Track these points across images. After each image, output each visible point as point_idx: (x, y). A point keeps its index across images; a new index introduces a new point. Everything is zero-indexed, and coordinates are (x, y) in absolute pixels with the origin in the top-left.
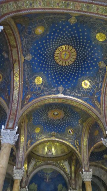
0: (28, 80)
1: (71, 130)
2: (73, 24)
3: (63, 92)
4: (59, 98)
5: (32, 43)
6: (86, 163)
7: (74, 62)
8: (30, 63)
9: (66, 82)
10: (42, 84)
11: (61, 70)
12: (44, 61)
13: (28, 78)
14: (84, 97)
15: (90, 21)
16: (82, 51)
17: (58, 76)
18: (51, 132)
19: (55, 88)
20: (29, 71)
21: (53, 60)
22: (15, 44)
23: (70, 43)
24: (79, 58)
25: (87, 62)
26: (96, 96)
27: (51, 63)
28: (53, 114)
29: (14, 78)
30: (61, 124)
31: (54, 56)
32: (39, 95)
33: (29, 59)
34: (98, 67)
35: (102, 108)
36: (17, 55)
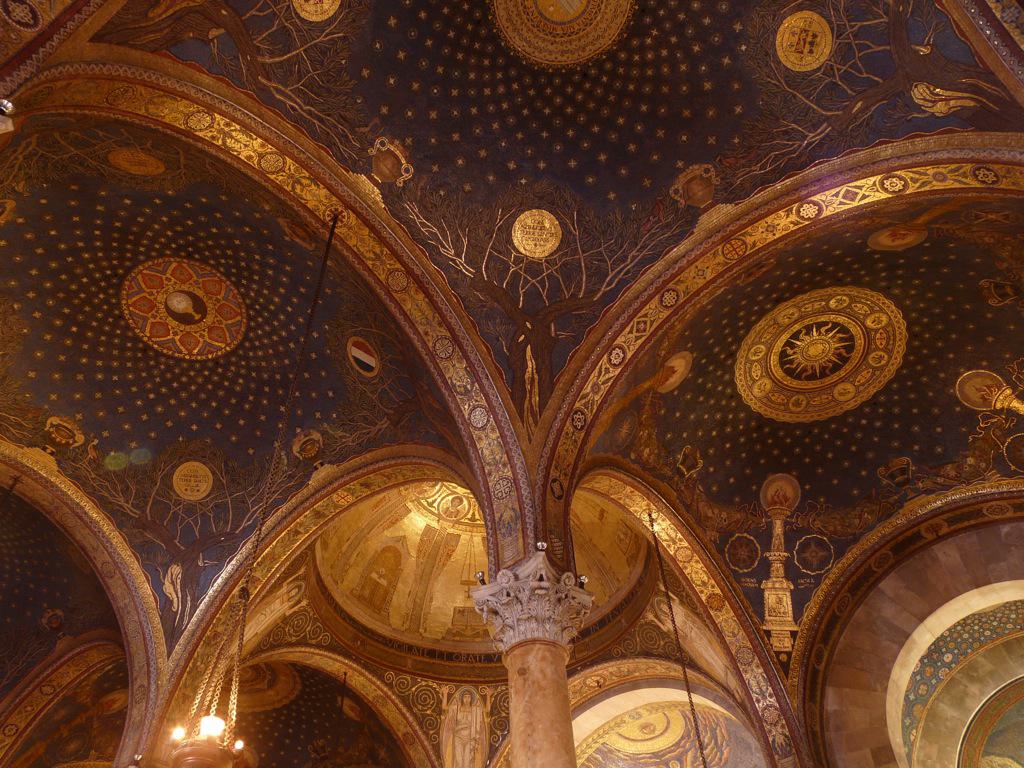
18: (287, 446)
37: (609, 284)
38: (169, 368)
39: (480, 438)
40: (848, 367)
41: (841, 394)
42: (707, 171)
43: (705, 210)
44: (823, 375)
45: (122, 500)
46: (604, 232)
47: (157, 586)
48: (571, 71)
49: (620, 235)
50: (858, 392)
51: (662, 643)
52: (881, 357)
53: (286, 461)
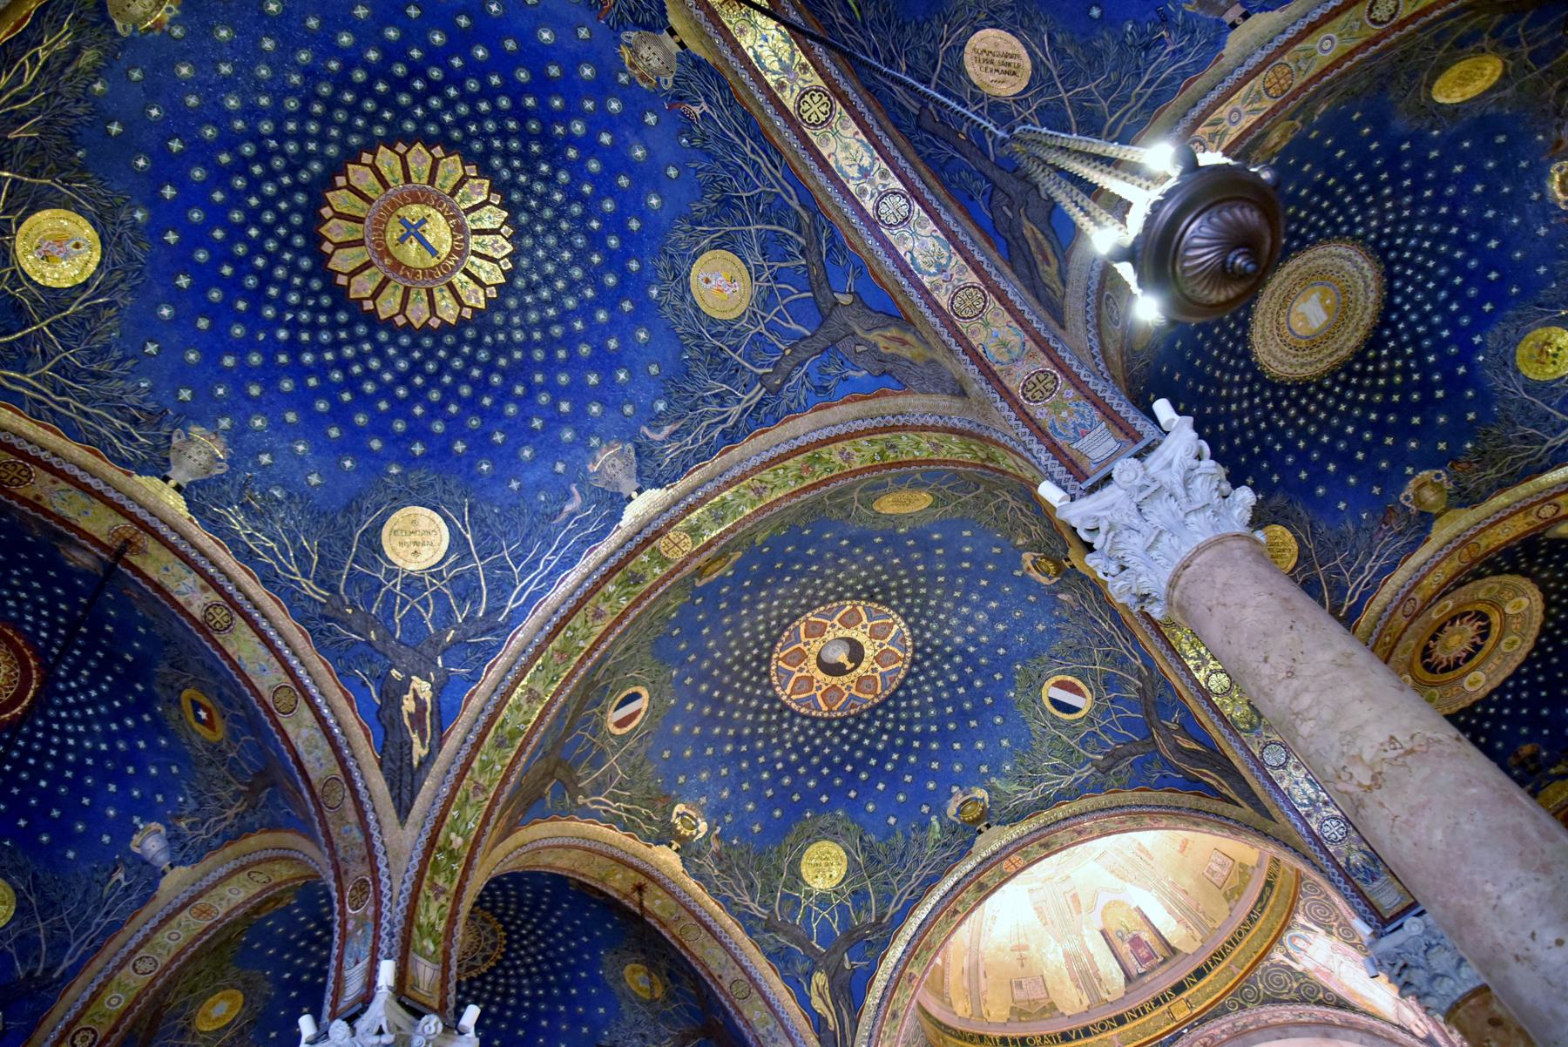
0: (333, 589)
1: (1061, 685)
3: (639, 473)
5: (117, 354)
6: (1357, 859)
9: (598, 395)
10: (457, 541)
11: (497, 350)
13: (321, 583)
14: (788, 379)
16: (463, 109)
17: (518, 400)
19: (568, 496)
21: (383, 336)
23: (342, 143)
24: (507, 165)
25: (570, 139)
26: (845, 299)
27: (388, 364)
28: (819, 675)
29: (230, 650)
30: (956, 701)
31: (360, 301)
32: (491, 630)
34: (652, 99)
36: (99, 506)
37: (1352, 598)
38: (803, 730)
39: (1282, 778)
40: (1479, 656)
41: (1471, 684)
42: (1438, 476)
43: (1439, 515)
44: (1457, 666)
45: (747, 898)
46: (1338, 544)
47: (804, 1002)
48: (1308, 383)
49: (1354, 546)
50: (1488, 680)
51: (1295, 985)
52: (1514, 642)
53: (938, 827)
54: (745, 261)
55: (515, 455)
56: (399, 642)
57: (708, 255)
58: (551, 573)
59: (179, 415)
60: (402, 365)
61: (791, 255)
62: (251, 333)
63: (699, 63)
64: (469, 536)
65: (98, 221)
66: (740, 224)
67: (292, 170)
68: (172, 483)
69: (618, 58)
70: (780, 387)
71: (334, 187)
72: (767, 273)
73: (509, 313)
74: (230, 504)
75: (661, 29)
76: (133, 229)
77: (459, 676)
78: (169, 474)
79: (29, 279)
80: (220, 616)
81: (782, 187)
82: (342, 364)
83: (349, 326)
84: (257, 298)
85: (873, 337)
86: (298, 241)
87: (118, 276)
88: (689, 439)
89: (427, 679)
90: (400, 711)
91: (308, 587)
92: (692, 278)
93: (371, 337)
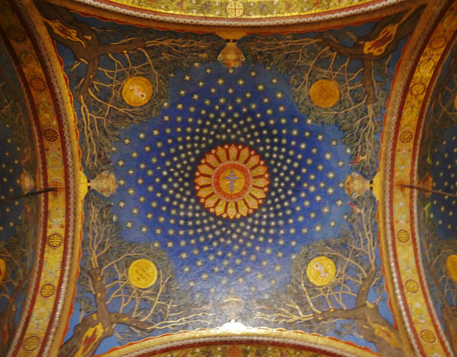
0: (101, 266)
2: (234, 68)
4: (226, 342)
5: (117, 133)
7: (265, 200)
8: (109, 206)
10: (156, 287)
11: (223, 235)
12: (161, 202)
13: (99, 260)
14: (325, 320)
15: (280, 50)
16: (282, 157)
20: (106, 232)
21: (193, 201)
22: (55, 123)
23: (238, 137)
27: (186, 210)
33: (108, 190)
34: (345, 197)
35: (404, 341)
36: (62, 168)
54: (337, 269)
55: (200, 274)
56: (106, 306)
57: (324, 258)
58: (179, 326)
59: (113, 167)
60: (190, 214)
61: (358, 278)
62: (157, 164)
63: (372, 198)
64: (161, 289)
65: (155, 95)
66: (345, 255)
67: (217, 132)
68: (89, 184)
69: (345, 179)
70: (320, 321)
71: (223, 147)
72: (342, 278)
73: (238, 226)
74: (98, 208)
75: (368, 179)
76: (160, 106)
77: (117, 338)
78: (91, 181)
79: (121, 90)
80: (56, 241)
81: (371, 254)
82: (173, 198)
83: (186, 189)
84: (169, 157)
85: (375, 326)
86: (197, 152)
87: (142, 114)
88: (269, 316)
89: (104, 328)
90: (84, 332)
91: (94, 257)
92: (312, 262)
93: (189, 198)
